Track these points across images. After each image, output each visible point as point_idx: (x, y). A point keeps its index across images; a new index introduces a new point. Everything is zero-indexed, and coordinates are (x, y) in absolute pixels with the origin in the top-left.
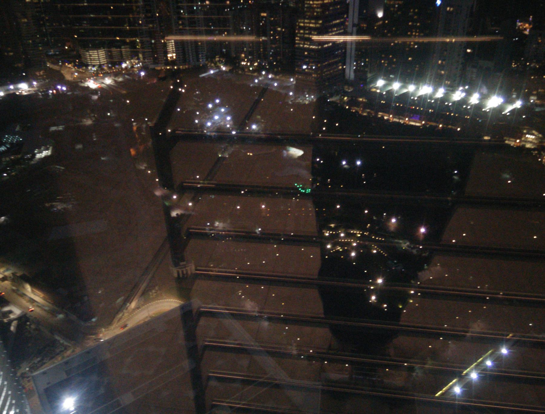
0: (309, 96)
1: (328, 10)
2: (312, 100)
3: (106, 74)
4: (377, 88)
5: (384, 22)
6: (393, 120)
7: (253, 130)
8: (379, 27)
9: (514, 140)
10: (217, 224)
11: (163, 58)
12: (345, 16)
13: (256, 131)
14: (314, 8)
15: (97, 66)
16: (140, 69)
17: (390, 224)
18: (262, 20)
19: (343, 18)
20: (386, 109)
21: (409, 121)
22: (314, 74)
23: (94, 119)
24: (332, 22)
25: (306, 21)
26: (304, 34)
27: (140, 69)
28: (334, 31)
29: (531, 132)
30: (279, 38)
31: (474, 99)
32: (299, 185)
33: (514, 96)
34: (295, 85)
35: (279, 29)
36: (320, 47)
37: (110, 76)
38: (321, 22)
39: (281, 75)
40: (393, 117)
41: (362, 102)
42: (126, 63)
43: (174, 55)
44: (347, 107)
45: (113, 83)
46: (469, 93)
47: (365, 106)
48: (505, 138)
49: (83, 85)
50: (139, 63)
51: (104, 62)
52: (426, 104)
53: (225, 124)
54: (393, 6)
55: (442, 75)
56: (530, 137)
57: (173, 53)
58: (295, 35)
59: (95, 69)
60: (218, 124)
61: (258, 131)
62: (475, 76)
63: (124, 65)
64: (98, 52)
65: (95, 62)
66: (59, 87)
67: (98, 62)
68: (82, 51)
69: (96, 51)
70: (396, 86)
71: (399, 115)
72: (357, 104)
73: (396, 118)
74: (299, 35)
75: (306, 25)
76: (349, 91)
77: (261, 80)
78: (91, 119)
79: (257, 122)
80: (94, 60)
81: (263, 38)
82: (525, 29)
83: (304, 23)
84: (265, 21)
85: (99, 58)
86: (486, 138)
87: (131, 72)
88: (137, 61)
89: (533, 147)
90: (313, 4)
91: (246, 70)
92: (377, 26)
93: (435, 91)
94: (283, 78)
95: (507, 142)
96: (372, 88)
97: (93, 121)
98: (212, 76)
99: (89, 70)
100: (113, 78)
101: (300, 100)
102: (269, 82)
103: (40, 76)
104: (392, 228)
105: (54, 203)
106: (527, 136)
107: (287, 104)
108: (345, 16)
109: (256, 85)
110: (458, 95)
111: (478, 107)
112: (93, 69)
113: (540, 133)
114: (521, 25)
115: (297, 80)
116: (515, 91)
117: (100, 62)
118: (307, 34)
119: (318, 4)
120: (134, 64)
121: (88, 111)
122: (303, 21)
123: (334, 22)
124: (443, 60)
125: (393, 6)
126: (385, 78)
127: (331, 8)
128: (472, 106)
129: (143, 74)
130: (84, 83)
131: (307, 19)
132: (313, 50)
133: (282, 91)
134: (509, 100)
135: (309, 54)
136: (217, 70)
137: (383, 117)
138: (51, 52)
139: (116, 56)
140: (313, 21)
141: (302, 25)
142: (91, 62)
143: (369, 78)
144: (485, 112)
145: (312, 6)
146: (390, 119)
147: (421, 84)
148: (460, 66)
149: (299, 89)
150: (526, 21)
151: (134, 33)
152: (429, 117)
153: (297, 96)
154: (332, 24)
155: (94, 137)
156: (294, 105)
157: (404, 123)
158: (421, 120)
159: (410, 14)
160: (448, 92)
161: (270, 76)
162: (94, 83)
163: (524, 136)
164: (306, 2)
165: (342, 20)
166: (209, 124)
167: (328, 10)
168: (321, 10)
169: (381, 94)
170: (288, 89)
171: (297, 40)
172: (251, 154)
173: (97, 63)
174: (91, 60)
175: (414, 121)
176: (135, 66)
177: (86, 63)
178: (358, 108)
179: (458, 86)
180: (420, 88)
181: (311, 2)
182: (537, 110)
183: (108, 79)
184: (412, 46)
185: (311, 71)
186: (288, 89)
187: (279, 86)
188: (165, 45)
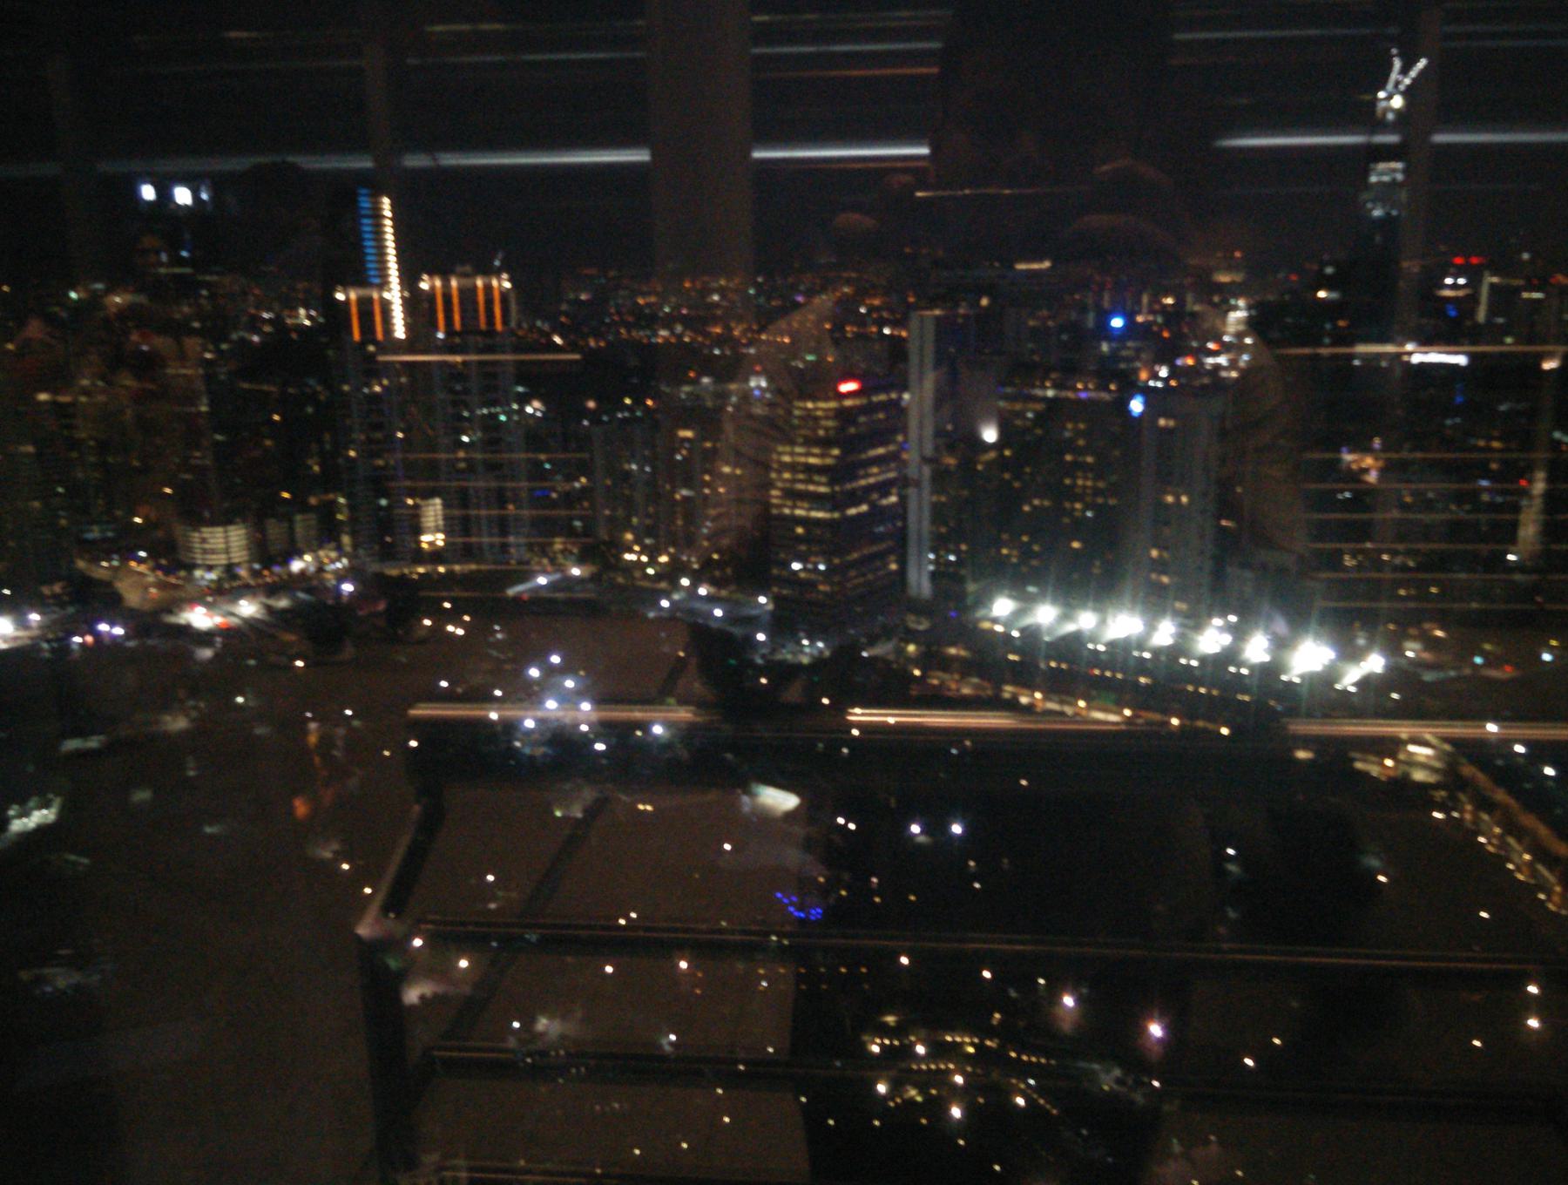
0: (812, 641)
1: (854, 423)
2: (821, 651)
4: (995, 621)
7: (656, 737)
8: (989, 464)
10: (542, 1023)
13: (663, 741)
14: (816, 419)
16: (342, 577)
17: (1060, 1012)
18: (682, 447)
19: (894, 442)
20: (1025, 675)
21: (1089, 708)
22: (822, 583)
23: (194, 714)
24: (865, 450)
25: (799, 450)
26: (794, 481)
27: (342, 577)
31: (1257, 649)
33: (1361, 642)
34: (773, 614)
36: (836, 515)
38: (836, 452)
39: (733, 587)
40: (1046, 698)
43: (441, 536)
46: (1239, 633)
48: (1354, 755)
49: (172, 619)
50: (338, 559)
54: (1021, 415)
55: (1163, 587)
57: (437, 530)
59: (213, 576)
63: (296, 566)
65: (214, 557)
66: (103, 627)
67: (224, 556)
68: (179, 529)
69: (220, 529)
70: (1045, 615)
72: (946, 664)
74: (779, 484)
76: (921, 628)
77: (679, 601)
78: (187, 716)
81: (685, 492)
82: (1366, 471)
83: (792, 454)
84: (690, 450)
87: (315, 583)
88: (333, 554)
90: (817, 409)
91: (637, 574)
93: (1151, 627)
94: (739, 596)
95: (1359, 765)
97: (192, 721)
101: (786, 655)
102: (698, 605)
103: (55, 596)
104: (1067, 1026)
105: (46, 971)
107: (752, 664)
109: (664, 614)
110: (1212, 639)
111: (1269, 672)
114: (1354, 461)
115: (777, 599)
118: (801, 481)
120: (326, 561)
121: (181, 694)
122: (788, 449)
124: (1160, 548)
125: (1021, 415)
126: (1014, 593)
128: (1252, 668)
129: (348, 588)
131: (802, 445)
132: (818, 522)
133: (737, 631)
134: (1351, 654)
136: (557, 576)
138: (92, 531)
140: (816, 451)
141: (787, 459)
142: (203, 559)
144: (1290, 684)
145: (813, 413)
147: (1110, 610)
148: (1208, 565)
149: (784, 624)
150: (1368, 450)
152: (1142, 699)
158: (1120, 705)
160: (1187, 631)
161: (703, 591)
165: (892, 448)
167: (854, 423)
169: (1007, 637)
170: (753, 623)
171: (777, 497)
172: (649, 808)
173: (221, 560)
174: (205, 551)
180: (1110, 621)
182: (1428, 677)
185: (813, 576)
186: (753, 623)
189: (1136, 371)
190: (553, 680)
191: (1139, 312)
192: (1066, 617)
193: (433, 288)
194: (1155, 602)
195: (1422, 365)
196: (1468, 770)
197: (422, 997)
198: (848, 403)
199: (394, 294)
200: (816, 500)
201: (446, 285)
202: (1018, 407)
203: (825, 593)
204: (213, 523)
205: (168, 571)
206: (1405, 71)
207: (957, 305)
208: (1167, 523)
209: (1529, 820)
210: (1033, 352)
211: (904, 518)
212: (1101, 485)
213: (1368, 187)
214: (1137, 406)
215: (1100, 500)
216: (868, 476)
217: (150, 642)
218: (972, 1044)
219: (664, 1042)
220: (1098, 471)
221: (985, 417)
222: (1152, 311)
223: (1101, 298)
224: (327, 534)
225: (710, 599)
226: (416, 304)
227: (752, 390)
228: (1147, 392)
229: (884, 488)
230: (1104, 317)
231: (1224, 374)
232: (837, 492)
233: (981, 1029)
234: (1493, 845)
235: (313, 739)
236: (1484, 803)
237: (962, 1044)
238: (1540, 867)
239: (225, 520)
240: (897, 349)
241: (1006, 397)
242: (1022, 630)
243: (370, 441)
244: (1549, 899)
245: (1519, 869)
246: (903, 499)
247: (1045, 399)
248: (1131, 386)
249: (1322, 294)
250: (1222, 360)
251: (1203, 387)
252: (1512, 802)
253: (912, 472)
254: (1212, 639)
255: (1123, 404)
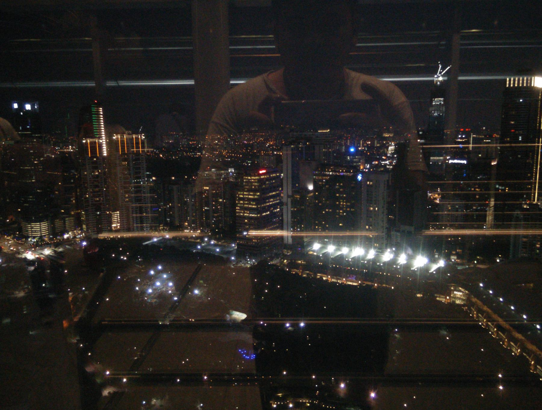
1: (265, 184)
3: (47, 245)
4: (314, 251)
5: (315, 194)
6: (331, 280)
9: (444, 297)
10: (154, 401)
11: (108, 228)
12: (280, 189)
15: (38, 238)
16: (82, 240)
17: (339, 390)
19: (278, 190)
21: (347, 281)
24: (269, 193)
25: (245, 193)
26: (244, 204)
27: (82, 240)
28: (271, 201)
29: (457, 289)
30: (221, 208)
31: (402, 259)
32: (243, 351)
33: (437, 256)
34: (237, 250)
35: (221, 200)
36: (259, 215)
37: (50, 247)
38: (259, 194)
40: (332, 278)
41: (301, 264)
42: (68, 233)
44: (287, 270)
45: (52, 254)
46: (397, 254)
47: (305, 268)
49: (20, 256)
50: (82, 233)
51: (46, 233)
52: (360, 264)
53: (167, 289)
56: (458, 294)
57: (118, 223)
58: (235, 205)
60: (160, 291)
61: (201, 295)
62: (399, 239)
63: (66, 236)
64: (40, 224)
69: (39, 223)
70: (331, 249)
71: (336, 276)
73: (334, 278)
74: (239, 205)
75: (245, 196)
77: (204, 246)
78: (24, 291)
79: (199, 287)
80: (35, 232)
82: (436, 199)
83: (243, 195)
84: (208, 194)
85: (41, 230)
86: (419, 295)
89: (462, 303)
92: (308, 197)
93: (367, 252)
94: (225, 244)
95: (438, 299)
96: (310, 251)
98: (156, 244)
99: (29, 242)
100: (54, 249)
102: (210, 247)
104: (342, 395)
106: (455, 292)
108: (280, 189)
110: (387, 256)
111: (407, 267)
112: (33, 241)
113: (466, 289)
114: (432, 196)
115: (238, 245)
116: (437, 252)
117: (41, 234)
118: (246, 204)
119: (256, 179)
122: (242, 193)
123: (270, 194)
127: (267, 182)
128: (401, 266)
130: (21, 255)
131: (246, 191)
132: (252, 218)
133: (225, 256)
134: (433, 260)
135: (249, 221)
137: (321, 277)
139: (59, 228)
141: (242, 196)
143: (306, 241)
144: (414, 271)
146: (329, 279)
147: (353, 246)
151: (78, 206)
153: (239, 259)
154: (269, 196)
155: (25, 309)
156: (235, 269)
157: (342, 283)
159: (337, 187)
161: (212, 243)
162: (32, 254)
163: (452, 292)
164: (244, 177)
165: (277, 192)
166: (150, 291)
167: (265, 184)
168: (258, 184)
169: (318, 257)
170: (230, 253)
174: (32, 232)
175: (351, 281)
176: (77, 237)
177: (26, 235)
178: (298, 270)
179: (386, 248)
181: (249, 178)
182: (459, 268)
183: (47, 250)
184: (341, 214)
187: (222, 252)
188: (110, 216)
189: (359, 166)
190: (160, 275)
191: (360, 147)
192: (338, 249)
193: (118, 138)
194: (368, 243)
195: (452, 163)
196: (474, 300)
197: (109, 393)
198: (262, 177)
199: (103, 141)
200: (251, 210)
201: (122, 138)
202: (320, 178)
203: (255, 242)
204: (35, 221)
205: (18, 239)
206: (443, 69)
207: (299, 144)
208: (371, 217)
209: (495, 317)
210: (324, 160)
211: (282, 216)
212: (349, 204)
213: (432, 106)
214: (360, 178)
215: (348, 209)
216: (269, 202)
217: (11, 265)
218: (309, 403)
219: (198, 406)
220: (347, 199)
221: (309, 182)
222: (363, 146)
223: (347, 142)
224: (78, 224)
225: (215, 245)
226: (111, 144)
227: (230, 173)
228: (363, 173)
229: (275, 206)
230: (348, 148)
231: (388, 167)
232: (259, 207)
233: (312, 397)
234: (484, 325)
235: (70, 299)
236: (480, 311)
237: (305, 403)
238: (499, 332)
239: (40, 220)
240: (279, 159)
241: (316, 175)
242: (323, 254)
243: (94, 192)
244: (503, 343)
245: (493, 333)
246: (281, 210)
247: (329, 175)
248: (357, 171)
249: (419, 141)
250: (387, 162)
251: (381, 171)
252: (490, 311)
253: (284, 200)
254: (387, 256)
255: (356, 176)
